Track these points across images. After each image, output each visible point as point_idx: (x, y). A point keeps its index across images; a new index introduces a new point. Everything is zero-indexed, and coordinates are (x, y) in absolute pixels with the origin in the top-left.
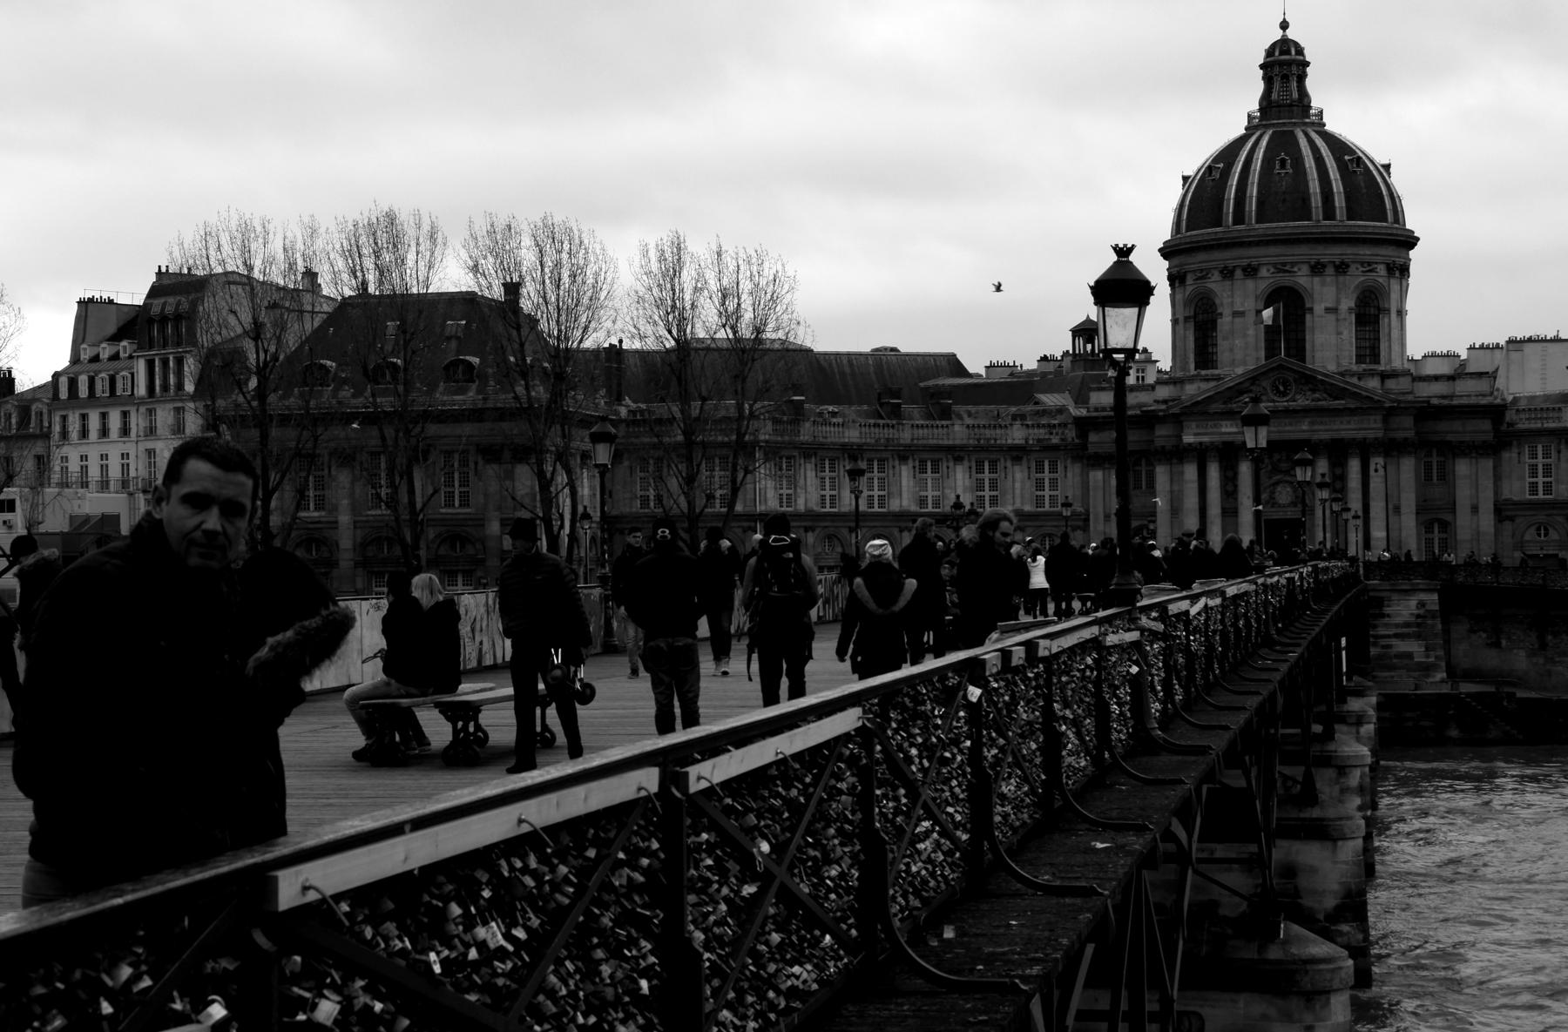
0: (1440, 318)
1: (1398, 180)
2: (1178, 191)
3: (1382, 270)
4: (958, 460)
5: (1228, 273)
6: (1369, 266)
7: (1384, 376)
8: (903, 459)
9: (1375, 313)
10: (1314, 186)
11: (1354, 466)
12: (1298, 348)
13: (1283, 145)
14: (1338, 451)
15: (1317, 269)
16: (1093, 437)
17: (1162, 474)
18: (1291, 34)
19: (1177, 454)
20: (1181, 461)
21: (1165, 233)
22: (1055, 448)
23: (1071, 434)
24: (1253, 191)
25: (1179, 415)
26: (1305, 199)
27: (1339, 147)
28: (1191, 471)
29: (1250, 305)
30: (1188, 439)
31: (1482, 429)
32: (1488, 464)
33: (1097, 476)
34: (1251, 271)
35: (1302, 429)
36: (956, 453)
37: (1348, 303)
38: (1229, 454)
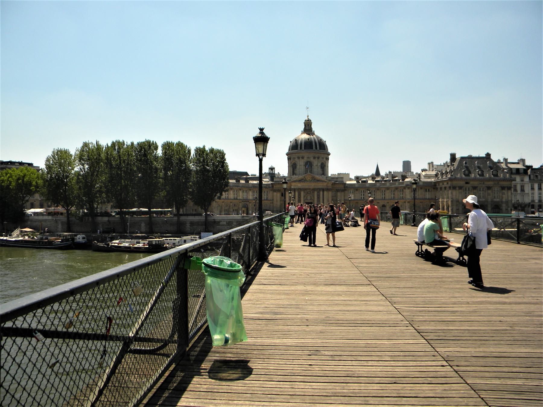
0: (334, 168)
1: (328, 144)
3: (325, 159)
4: (250, 190)
5: (299, 158)
6: (323, 158)
8: (240, 190)
9: (324, 167)
10: (314, 144)
11: (321, 193)
14: (319, 190)
15: (314, 158)
21: (287, 151)
23: (271, 186)
26: (312, 146)
30: (292, 187)
31: (342, 187)
32: (343, 193)
33: (275, 194)
34: (303, 158)
35: (313, 185)
37: (319, 164)
38: (300, 190)
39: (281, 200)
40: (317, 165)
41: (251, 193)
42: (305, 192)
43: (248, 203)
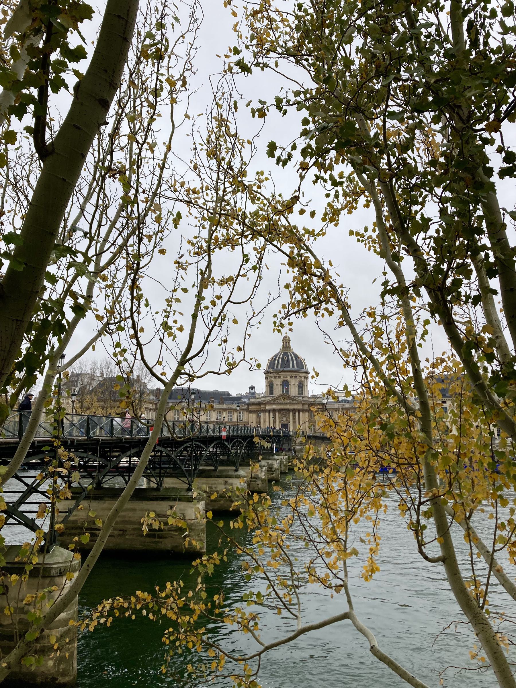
5: (275, 377)
6: (301, 377)
13: (286, 354)
14: (294, 410)
15: (291, 377)
19: (265, 411)
23: (246, 407)
27: (296, 355)
28: (267, 414)
34: (279, 377)
35: (288, 407)
36: (224, 410)
37: (297, 383)
38: (274, 411)
41: (225, 414)
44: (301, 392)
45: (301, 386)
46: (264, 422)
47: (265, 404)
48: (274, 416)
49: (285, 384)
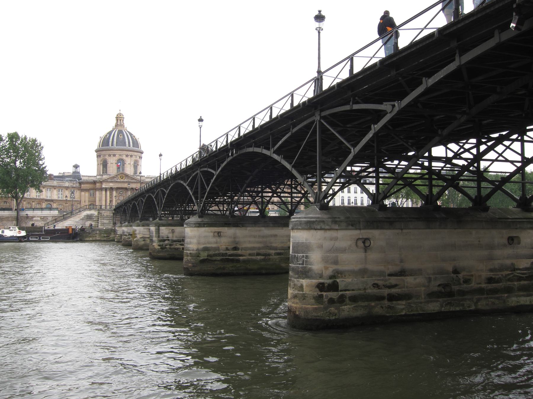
1: (141, 141)
2: (99, 140)
4: (55, 189)
7: (141, 176)
10: (127, 141)
12: (123, 169)
15: (127, 156)
16: (82, 186)
17: (97, 193)
18: (121, 112)
19: (101, 189)
20: (102, 191)
21: (96, 147)
22: (74, 187)
23: (78, 185)
24: (115, 140)
25: (101, 182)
26: (125, 143)
27: (131, 134)
28: (104, 192)
29: (114, 162)
33: (83, 193)
34: (114, 155)
35: (126, 185)
36: (54, 187)
37: (132, 163)
38: (111, 189)
39: (89, 201)
40: (130, 164)
41: (55, 192)
42: (116, 192)
43: (52, 203)
44: (135, 173)
45: (136, 165)
46: (100, 200)
47: (101, 182)
48: (111, 195)
49: (121, 163)
